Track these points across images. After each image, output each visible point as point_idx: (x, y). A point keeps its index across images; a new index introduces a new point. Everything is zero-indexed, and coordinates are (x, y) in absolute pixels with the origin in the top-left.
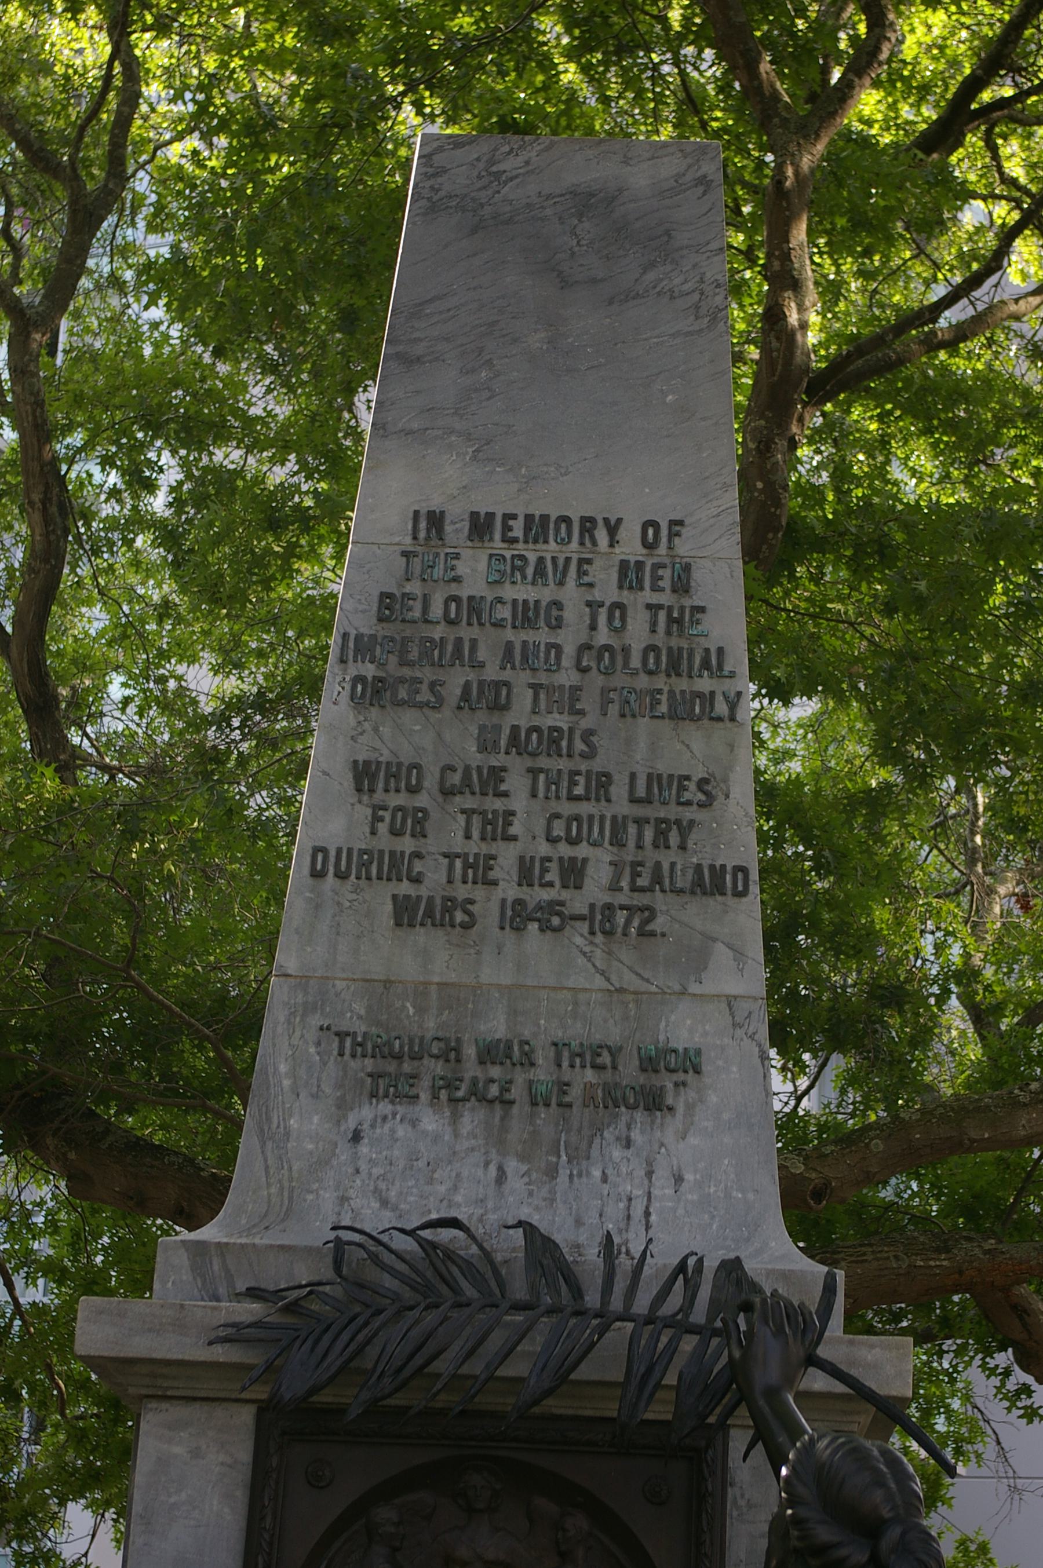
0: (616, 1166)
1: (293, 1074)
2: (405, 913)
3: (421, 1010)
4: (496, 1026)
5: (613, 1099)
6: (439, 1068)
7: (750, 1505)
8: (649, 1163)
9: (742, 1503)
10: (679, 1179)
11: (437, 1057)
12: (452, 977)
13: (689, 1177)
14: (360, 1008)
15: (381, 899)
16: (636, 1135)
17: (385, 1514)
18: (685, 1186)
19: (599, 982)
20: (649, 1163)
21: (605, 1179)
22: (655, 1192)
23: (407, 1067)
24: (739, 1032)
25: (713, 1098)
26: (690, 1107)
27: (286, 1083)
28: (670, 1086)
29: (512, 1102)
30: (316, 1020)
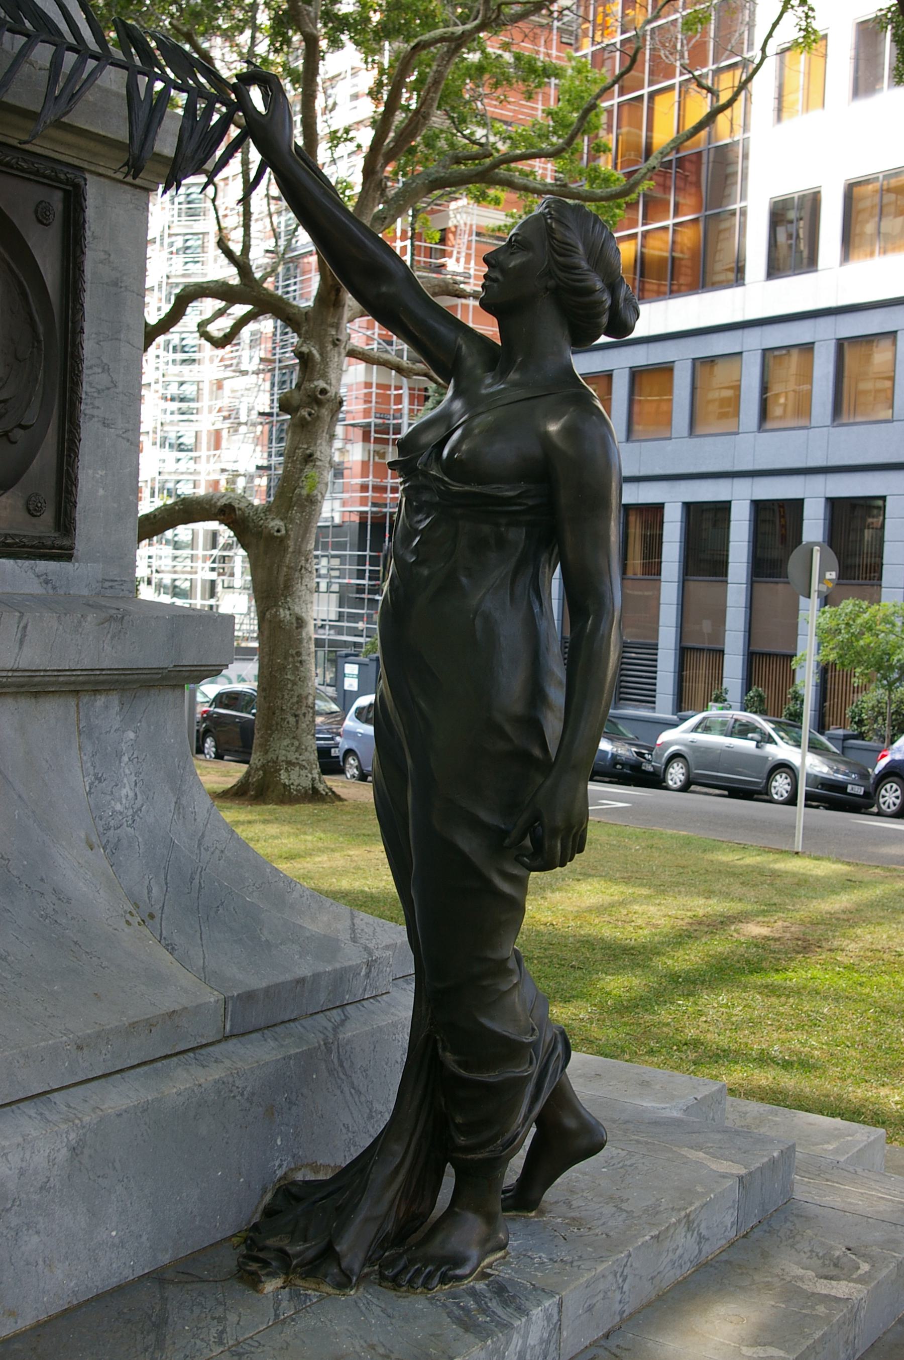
7: (94, 238)
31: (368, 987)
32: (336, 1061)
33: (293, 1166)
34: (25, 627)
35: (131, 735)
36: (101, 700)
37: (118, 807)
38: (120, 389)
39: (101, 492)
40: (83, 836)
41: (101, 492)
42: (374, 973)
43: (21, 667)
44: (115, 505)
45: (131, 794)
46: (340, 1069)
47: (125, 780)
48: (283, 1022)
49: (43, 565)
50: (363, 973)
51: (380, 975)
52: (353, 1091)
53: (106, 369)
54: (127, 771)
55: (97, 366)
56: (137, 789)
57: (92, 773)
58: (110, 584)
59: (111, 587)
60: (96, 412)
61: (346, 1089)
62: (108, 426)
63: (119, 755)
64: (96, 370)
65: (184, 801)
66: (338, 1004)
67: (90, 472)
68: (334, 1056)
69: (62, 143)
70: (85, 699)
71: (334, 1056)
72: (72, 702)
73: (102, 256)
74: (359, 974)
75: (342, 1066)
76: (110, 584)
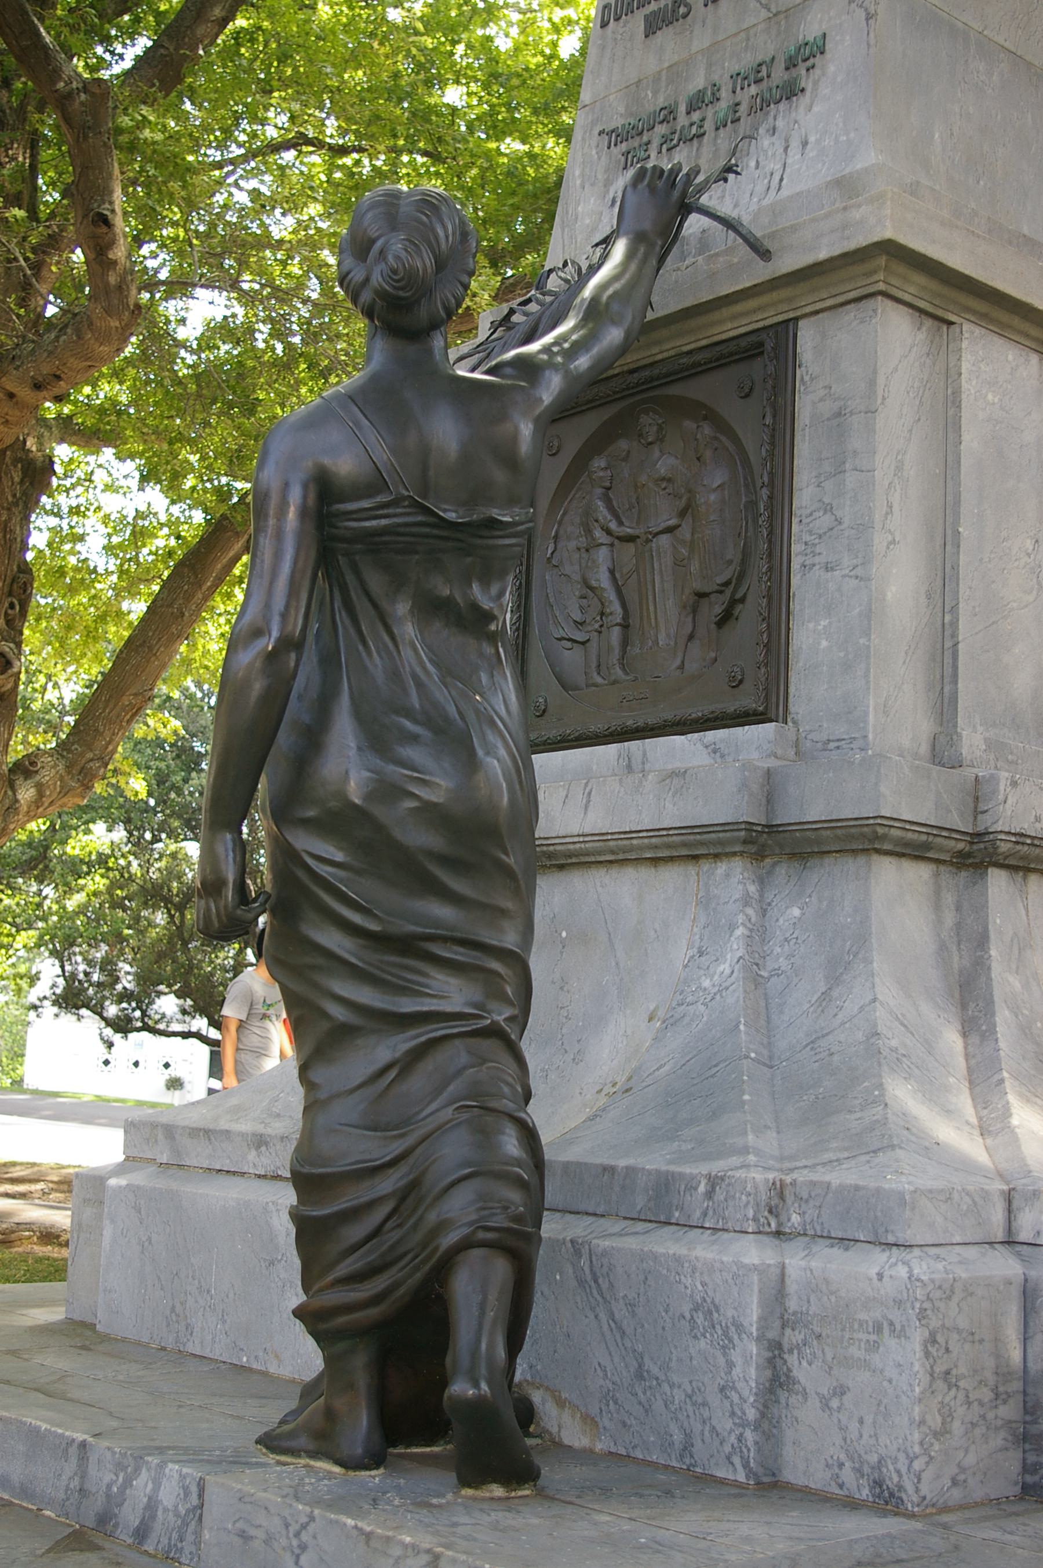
0: (765, 151)
1: (582, 175)
2: (652, 26)
3: (655, 93)
4: (698, 82)
5: (763, 104)
6: (661, 129)
8: (787, 141)
9: (807, 378)
10: (805, 144)
11: (661, 122)
12: (676, 58)
13: (812, 139)
14: (622, 109)
15: (637, 22)
16: (780, 123)
17: (599, 463)
18: (809, 146)
19: (764, 14)
20: (787, 141)
21: (757, 167)
22: (789, 161)
23: (645, 139)
24: (853, 5)
25: (832, 68)
26: (816, 83)
27: (578, 182)
28: (804, 72)
29: (704, 134)
30: (596, 132)
31: (711, 1213)
32: (587, 1271)
33: (529, 1378)
34: (590, 793)
35: (796, 912)
36: (722, 868)
37: (706, 983)
38: (846, 522)
39: (824, 644)
40: (652, 1008)
41: (824, 644)
42: (720, 1195)
43: (587, 831)
44: (842, 654)
45: (728, 971)
46: (593, 1284)
47: (729, 956)
48: (595, 1215)
49: (711, 735)
50: (702, 1188)
51: (731, 1203)
52: (613, 1325)
53: (828, 509)
54: (735, 947)
55: (818, 510)
56: (737, 967)
57: (697, 945)
58: (836, 744)
59: (838, 748)
60: (817, 559)
61: (603, 1316)
62: (832, 569)
63: (732, 927)
64: (816, 514)
65: (835, 993)
66: (662, 1218)
67: (811, 625)
68: (584, 1262)
69: (754, 311)
70: (705, 866)
71: (584, 1262)
72: (691, 869)
73: (822, 393)
74: (696, 1189)
75: (596, 1281)
76: (836, 744)
